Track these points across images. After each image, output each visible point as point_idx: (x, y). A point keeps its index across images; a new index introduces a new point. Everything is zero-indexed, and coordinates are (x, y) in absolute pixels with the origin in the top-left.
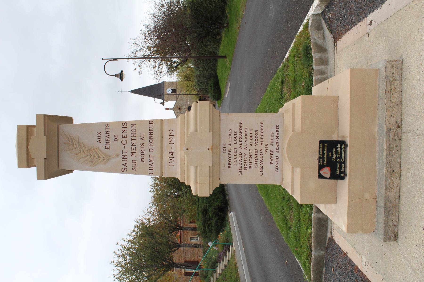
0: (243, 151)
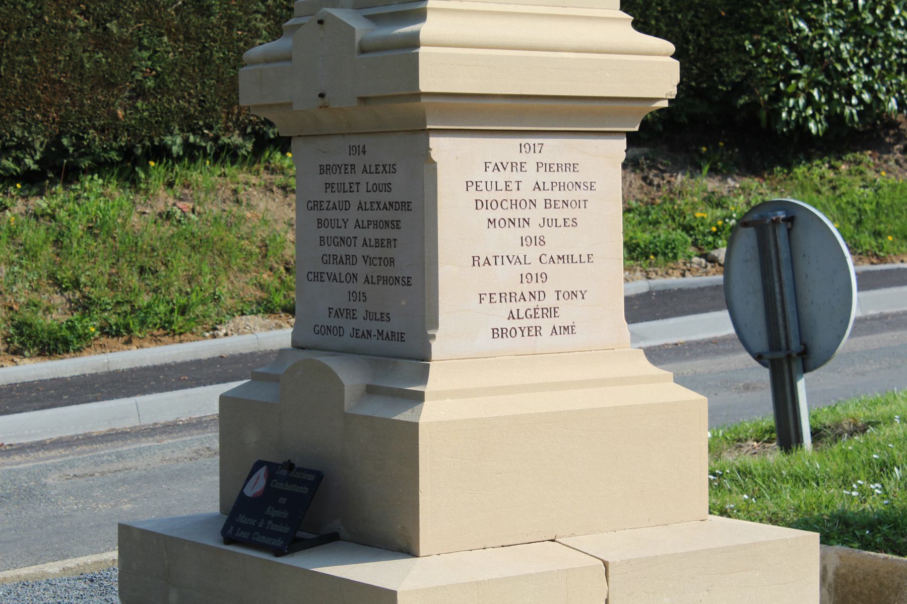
0: (353, 215)
